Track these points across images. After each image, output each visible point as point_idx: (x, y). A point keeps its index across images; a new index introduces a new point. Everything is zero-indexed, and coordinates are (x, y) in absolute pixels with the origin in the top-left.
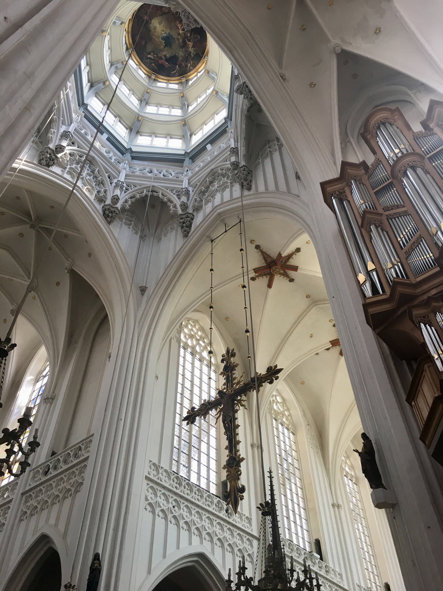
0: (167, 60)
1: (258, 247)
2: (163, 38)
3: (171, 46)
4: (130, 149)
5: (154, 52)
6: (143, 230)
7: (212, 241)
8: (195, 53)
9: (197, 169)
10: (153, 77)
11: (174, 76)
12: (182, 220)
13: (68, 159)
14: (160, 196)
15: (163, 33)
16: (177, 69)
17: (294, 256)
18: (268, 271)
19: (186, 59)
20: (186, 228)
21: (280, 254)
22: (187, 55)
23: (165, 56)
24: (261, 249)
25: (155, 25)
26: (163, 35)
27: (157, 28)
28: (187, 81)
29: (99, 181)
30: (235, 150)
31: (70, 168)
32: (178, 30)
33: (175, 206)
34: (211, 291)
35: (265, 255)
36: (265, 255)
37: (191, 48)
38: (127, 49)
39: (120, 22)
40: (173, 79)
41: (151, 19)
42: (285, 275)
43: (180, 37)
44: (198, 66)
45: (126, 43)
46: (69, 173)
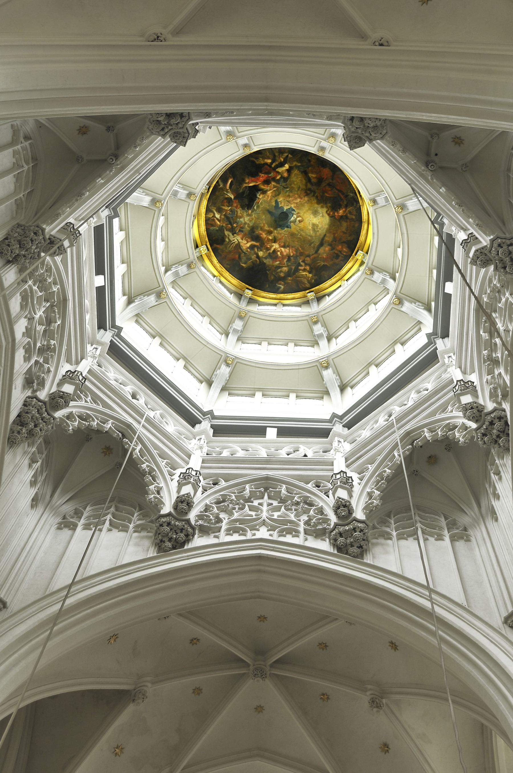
0: (255, 189)
3: (270, 212)
5: (285, 179)
8: (227, 240)
11: (224, 178)
15: (298, 219)
16: (228, 192)
19: (230, 219)
22: (235, 225)
23: (264, 192)
25: (319, 217)
26: (295, 216)
27: (312, 216)
32: (282, 244)
37: (240, 241)
43: (269, 240)
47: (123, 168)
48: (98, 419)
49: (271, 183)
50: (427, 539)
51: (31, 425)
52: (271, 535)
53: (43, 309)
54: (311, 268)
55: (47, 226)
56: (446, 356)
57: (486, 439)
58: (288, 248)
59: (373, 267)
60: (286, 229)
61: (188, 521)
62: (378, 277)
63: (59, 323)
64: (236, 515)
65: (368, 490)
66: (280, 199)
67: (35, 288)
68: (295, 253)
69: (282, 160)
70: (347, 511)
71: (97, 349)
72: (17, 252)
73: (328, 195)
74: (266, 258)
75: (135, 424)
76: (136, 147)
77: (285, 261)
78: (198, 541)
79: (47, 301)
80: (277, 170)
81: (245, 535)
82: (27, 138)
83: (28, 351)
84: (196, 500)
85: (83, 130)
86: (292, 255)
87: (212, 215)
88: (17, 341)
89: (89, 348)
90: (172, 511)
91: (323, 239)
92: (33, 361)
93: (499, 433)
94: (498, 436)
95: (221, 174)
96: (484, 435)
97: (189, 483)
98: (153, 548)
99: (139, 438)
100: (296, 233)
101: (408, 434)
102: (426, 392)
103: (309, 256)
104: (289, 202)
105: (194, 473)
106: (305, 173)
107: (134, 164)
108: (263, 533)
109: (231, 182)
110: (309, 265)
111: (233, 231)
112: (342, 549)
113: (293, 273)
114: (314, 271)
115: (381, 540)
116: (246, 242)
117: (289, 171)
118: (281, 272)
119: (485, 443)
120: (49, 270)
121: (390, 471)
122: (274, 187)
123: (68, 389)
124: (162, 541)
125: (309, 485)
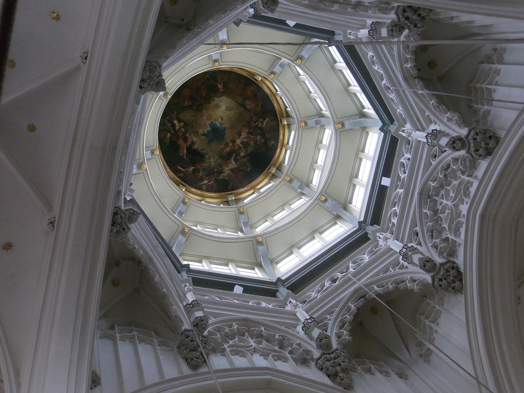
0: (190, 149)
2: (212, 125)
3: (210, 141)
5: (186, 125)
8: (226, 178)
11: (176, 171)
15: (220, 120)
16: (188, 170)
19: (210, 173)
22: (216, 170)
26: (217, 123)
27: (219, 110)
32: (238, 136)
37: (229, 168)
41: (223, 94)
43: (231, 146)
44: (213, 195)
47: (150, 259)
48: (346, 314)
49: (187, 137)
50: (497, 82)
51: (338, 368)
52: (467, 203)
53: (250, 339)
55: (183, 326)
56: (349, 36)
57: (419, 25)
58: (242, 132)
59: (269, 72)
60: (226, 131)
61: (442, 265)
62: (277, 69)
63: (263, 329)
64: (445, 225)
65: (445, 120)
66: (201, 131)
67: (231, 342)
68: (246, 128)
69: (169, 124)
70: (459, 141)
71: (290, 302)
72: (198, 354)
73: (205, 94)
74: (247, 151)
75: (356, 286)
76: (135, 248)
77: (252, 136)
78: (460, 260)
79: (243, 335)
80: (177, 130)
81: (463, 222)
82: (112, 328)
83: (279, 358)
84: (427, 254)
85: (115, 283)
86: (247, 130)
87: (204, 186)
88: (270, 366)
89: (289, 308)
90: (431, 274)
91: (239, 104)
92: (289, 356)
93: (416, 14)
94: (419, 15)
95: (172, 174)
96: (416, 26)
97: (411, 256)
98: (458, 296)
99: (366, 286)
100: (230, 124)
101: (406, 79)
102: (375, 57)
103: (251, 117)
104: (204, 125)
105: (404, 250)
106: (184, 108)
107: (148, 249)
108: (464, 208)
112: (489, 152)
113: (263, 132)
115: (489, 118)
116: (231, 164)
117: (179, 121)
118: (260, 141)
119: (423, 26)
120: (219, 330)
121: (433, 100)
122: (191, 135)
123: (316, 332)
124: (454, 288)
125: (433, 163)
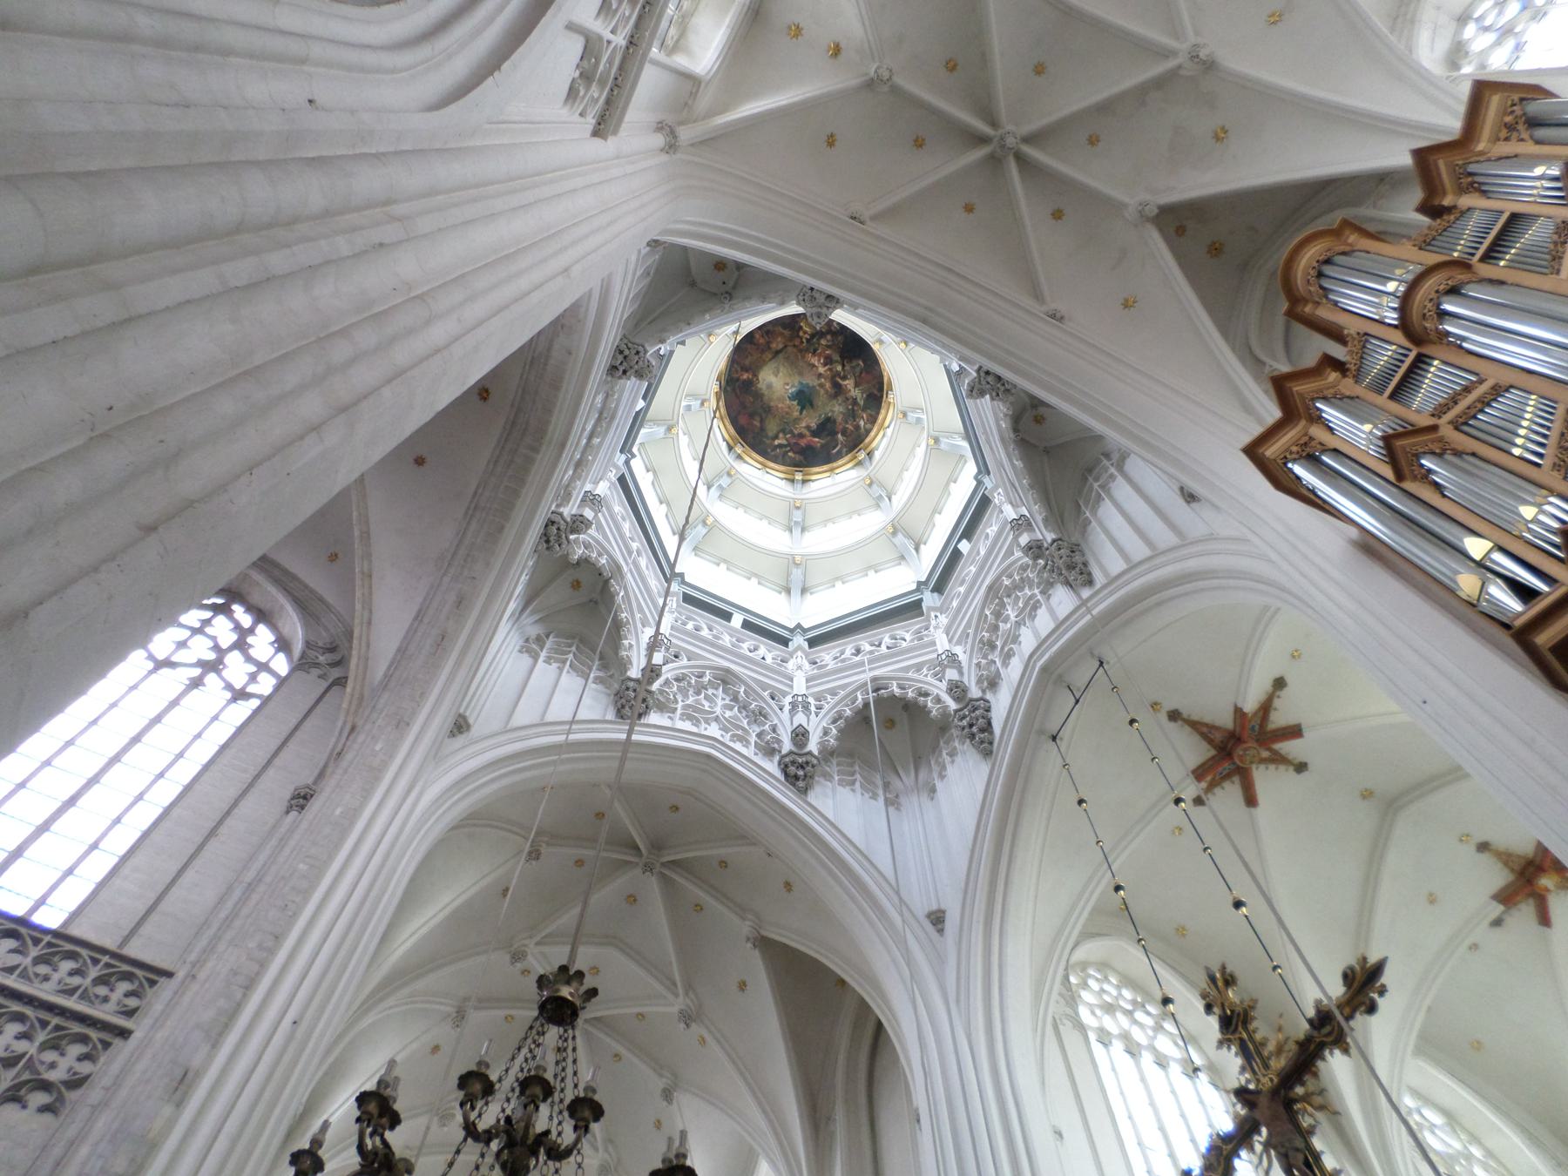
0: (815, 434)
1: (1174, 716)
2: (792, 398)
3: (812, 405)
4: (799, 626)
5: (783, 431)
6: (886, 786)
7: (1054, 738)
9: (955, 604)
10: (799, 477)
11: (839, 456)
12: (965, 722)
13: (675, 689)
14: (897, 691)
17: (1277, 703)
18: (1226, 766)
19: (852, 415)
20: (982, 736)
21: (1239, 712)
23: (808, 427)
24: (1185, 716)
28: (870, 455)
29: (753, 712)
30: (1020, 522)
31: (686, 707)
33: (938, 700)
34: (1106, 865)
35: (1201, 729)
36: (1201, 729)
38: (730, 448)
39: (699, 402)
40: (840, 462)
41: (755, 375)
42: (1279, 759)
44: (881, 417)
45: (724, 440)
46: (686, 717)
54: (798, 331)
74: (837, 362)
91: (773, 358)
103: (794, 346)
106: (762, 429)
109: (834, 448)
110: (798, 336)
111: (855, 402)
114: (797, 327)
117: (776, 437)
